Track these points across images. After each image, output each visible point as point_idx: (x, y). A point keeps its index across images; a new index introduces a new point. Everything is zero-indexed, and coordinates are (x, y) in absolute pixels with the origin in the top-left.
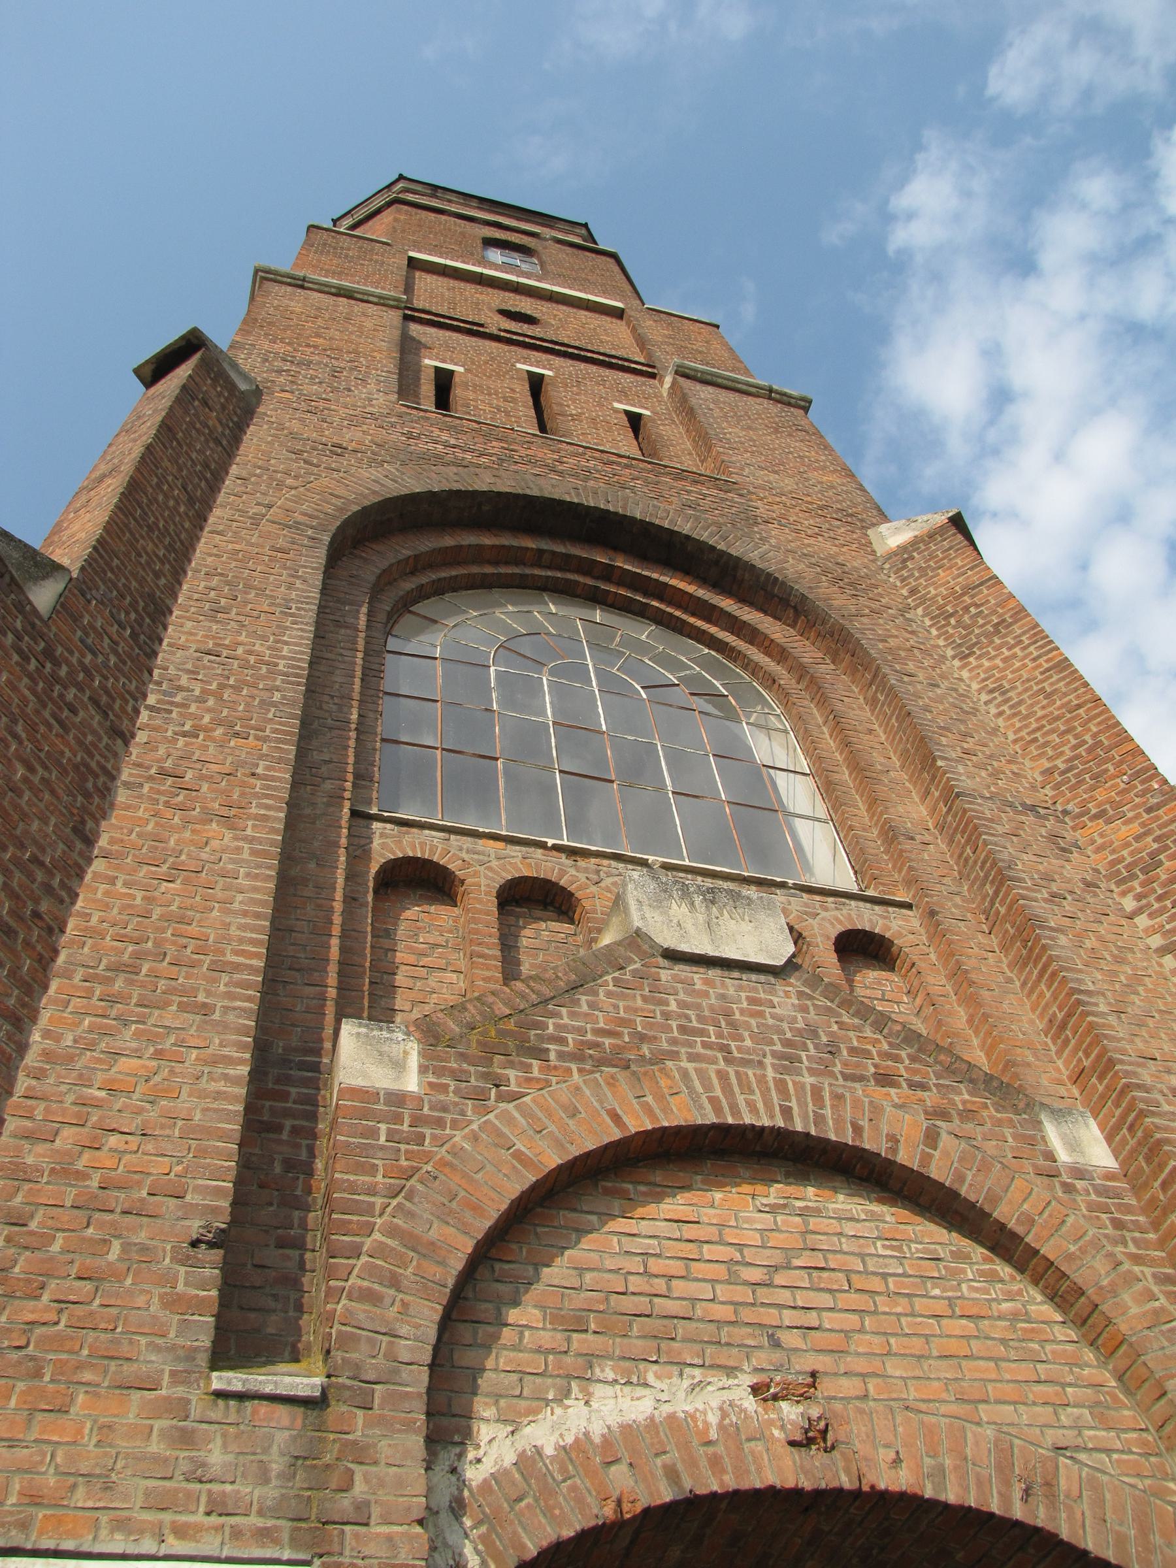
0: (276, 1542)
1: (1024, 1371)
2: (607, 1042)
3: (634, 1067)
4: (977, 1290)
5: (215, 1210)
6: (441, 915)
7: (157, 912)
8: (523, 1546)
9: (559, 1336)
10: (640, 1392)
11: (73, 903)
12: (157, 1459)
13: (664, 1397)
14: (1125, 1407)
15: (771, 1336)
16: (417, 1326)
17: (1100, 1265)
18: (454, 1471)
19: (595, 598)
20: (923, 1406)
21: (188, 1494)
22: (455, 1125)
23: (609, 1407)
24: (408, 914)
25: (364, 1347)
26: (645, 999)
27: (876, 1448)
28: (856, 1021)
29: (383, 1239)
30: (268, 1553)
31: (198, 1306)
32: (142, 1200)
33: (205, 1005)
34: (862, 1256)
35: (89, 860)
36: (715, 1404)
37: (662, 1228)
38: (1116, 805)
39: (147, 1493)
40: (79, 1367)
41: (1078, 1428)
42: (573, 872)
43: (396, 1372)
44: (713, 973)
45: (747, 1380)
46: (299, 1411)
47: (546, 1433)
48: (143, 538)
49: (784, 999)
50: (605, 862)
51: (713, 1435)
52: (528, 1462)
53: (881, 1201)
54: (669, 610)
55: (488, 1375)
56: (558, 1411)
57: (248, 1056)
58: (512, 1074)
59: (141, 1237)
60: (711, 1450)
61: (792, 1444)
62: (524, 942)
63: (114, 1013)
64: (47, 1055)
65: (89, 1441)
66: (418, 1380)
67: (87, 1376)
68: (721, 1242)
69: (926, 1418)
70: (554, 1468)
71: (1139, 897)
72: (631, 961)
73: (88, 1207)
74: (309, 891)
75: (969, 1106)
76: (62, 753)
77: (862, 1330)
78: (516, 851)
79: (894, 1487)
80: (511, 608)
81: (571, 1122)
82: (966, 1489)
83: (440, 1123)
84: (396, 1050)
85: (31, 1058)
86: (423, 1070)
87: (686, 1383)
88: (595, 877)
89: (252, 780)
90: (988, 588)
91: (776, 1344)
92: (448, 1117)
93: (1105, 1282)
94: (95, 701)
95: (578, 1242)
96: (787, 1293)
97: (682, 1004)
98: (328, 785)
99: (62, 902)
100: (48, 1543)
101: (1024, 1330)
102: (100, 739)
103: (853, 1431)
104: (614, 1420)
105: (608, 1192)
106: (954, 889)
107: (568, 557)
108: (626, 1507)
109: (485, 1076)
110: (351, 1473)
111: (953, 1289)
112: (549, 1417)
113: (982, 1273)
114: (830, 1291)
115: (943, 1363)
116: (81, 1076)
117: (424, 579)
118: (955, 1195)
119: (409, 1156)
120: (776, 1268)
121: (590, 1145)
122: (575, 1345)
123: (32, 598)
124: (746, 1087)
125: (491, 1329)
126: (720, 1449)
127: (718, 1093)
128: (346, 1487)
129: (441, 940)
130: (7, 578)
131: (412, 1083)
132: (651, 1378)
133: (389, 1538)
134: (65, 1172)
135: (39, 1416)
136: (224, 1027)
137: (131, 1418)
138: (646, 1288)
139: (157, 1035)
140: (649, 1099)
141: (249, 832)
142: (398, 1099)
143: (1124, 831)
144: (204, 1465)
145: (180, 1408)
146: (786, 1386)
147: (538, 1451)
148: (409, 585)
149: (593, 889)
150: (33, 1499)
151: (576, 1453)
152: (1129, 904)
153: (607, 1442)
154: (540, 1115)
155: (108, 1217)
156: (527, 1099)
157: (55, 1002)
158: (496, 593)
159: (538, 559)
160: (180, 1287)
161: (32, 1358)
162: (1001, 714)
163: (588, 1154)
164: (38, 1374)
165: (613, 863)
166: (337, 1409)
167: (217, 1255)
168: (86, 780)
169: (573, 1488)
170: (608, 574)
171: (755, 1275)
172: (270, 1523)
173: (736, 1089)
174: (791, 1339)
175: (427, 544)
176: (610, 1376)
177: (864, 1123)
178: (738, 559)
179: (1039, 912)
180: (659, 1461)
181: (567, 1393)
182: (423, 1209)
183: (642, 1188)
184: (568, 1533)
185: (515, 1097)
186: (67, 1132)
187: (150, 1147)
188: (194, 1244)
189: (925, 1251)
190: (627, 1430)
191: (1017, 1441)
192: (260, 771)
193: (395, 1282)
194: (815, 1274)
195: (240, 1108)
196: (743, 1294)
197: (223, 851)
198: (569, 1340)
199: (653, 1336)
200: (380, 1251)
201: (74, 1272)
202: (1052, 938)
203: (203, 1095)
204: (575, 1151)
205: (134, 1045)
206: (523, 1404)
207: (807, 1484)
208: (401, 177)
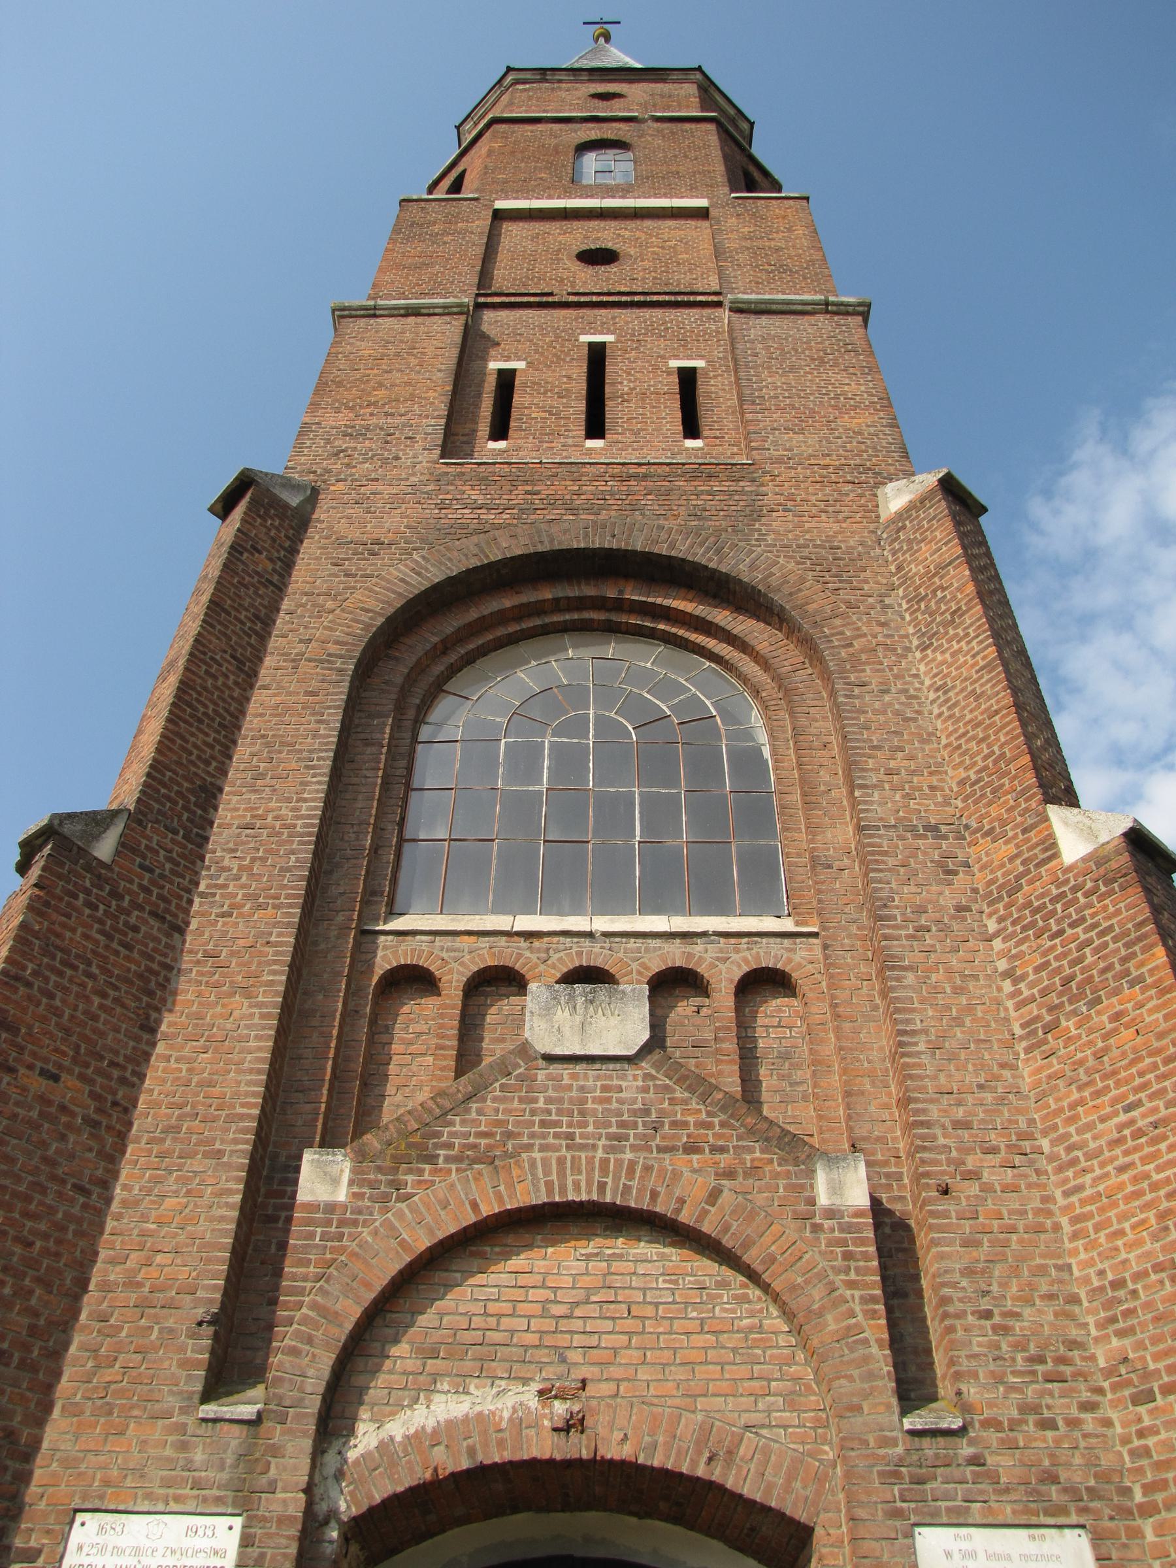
0: (224, 1504)
1: (743, 1371)
2: (483, 1142)
3: (497, 1162)
4: (726, 1310)
5: (211, 1301)
6: (429, 1005)
7: (195, 1079)
8: (373, 1497)
9: (419, 1362)
10: (463, 1397)
11: (143, 1082)
12: (169, 1459)
13: (478, 1400)
14: (815, 1394)
15: (561, 1355)
16: (318, 1370)
17: (817, 1292)
18: (340, 1453)
19: (612, 629)
20: (655, 1401)
21: (182, 1478)
22: (366, 1224)
23: (445, 1408)
24: (406, 1009)
25: (287, 1385)
26: (521, 1100)
27: (612, 1430)
28: (686, 1094)
29: (310, 1313)
30: (219, 1510)
31: (195, 1364)
32: (172, 1298)
33: (219, 1151)
34: (644, 1290)
35: (154, 1045)
36: (510, 1404)
37: (505, 1279)
38: (1003, 823)
39: (162, 1479)
40: (132, 1407)
41: (769, 1412)
42: (527, 954)
43: (303, 1399)
44: (579, 1068)
45: (535, 1387)
46: (245, 1427)
47: (397, 1428)
48: (193, 734)
49: (631, 1082)
50: (555, 940)
51: (504, 1425)
52: (384, 1446)
53: (673, 1244)
54: (674, 630)
55: (371, 1391)
56: (409, 1412)
57: (241, 1187)
58: (410, 1178)
59: (170, 1323)
60: (500, 1435)
61: (555, 1430)
62: (488, 1019)
63: (164, 1166)
64: (125, 1203)
65: (135, 1450)
66: (313, 1405)
67: (135, 1412)
68: (544, 1286)
69: (654, 1409)
70: (400, 1450)
71: (1000, 920)
72: (518, 1066)
73: (143, 1305)
74: (315, 1022)
75: (756, 1164)
76: (129, 970)
77: (628, 1347)
78: (484, 942)
79: (617, 1457)
80: (533, 663)
81: (442, 1213)
82: (668, 1457)
83: (355, 1223)
84: (335, 1169)
85: (115, 1207)
86: (351, 1183)
87: (495, 1390)
88: (544, 955)
89: (266, 949)
90: (955, 568)
91: (563, 1360)
92: (361, 1218)
93: (816, 1306)
94: (153, 914)
95: (445, 1294)
96: (580, 1322)
97: (549, 1100)
98: (340, 918)
99: (133, 1085)
100: (112, 1507)
101: (754, 1340)
102: (159, 942)
103: (599, 1423)
104: (442, 1417)
105: (473, 1255)
106: (854, 916)
107: (581, 599)
108: (440, 1472)
109: (391, 1183)
110: (269, 1463)
111: (708, 1311)
112: (402, 1416)
113: (735, 1297)
114: (613, 1318)
115: (682, 1368)
116: (142, 1215)
117: (452, 657)
118: (719, 1243)
119: (333, 1250)
120: (578, 1304)
121: (452, 1230)
122: (427, 1368)
123: (96, 854)
124: (576, 1169)
125: (376, 1360)
126: (507, 1435)
127: (554, 1177)
128: (266, 1471)
129: (425, 1028)
130: (75, 849)
131: (342, 1195)
132: (472, 1389)
133: (284, 1501)
134: (132, 1284)
135: (111, 1437)
136: (228, 1166)
137: (157, 1436)
138: (483, 1325)
139: (188, 1178)
140: (502, 1188)
141: (260, 999)
142: (331, 1207)
143: (1005, 850)
144: (191, 1461)
145: (182, 1428)
146: (563, 1389)
147: (392, 1438)
148: (438, 669)
149: (542, 967)
150: (106, 1483)
151: (415, 1439)
152: (992, 926)
153: (435, 1431)
154: (423, 1210)
155: (152, 1311)
156: (416, 1198)
157: (129, 1162)
158: (523, 648)
159: (557, 605)
160: (189, 1353)
161: (108, 1404)
162: (940, 715)
163: (452, 1236)
164: (110, 1413)
165: (562, 939)
166: (267, 1424)
167: (212, 1329)
168: (150, 981)
169: (409, 1462)
170: (620, 605)
171: (558, 1310)
172: (223, 1493)
173: (569, 1172)
174: (574, 1356)
175: (451, 624)
176: (446, 1387)
177: (661, 1190)
178: (727, 575)
179: (896, 951)
180: (465, 1444)
181: (416, 1400)
182: (334, 1288)
183: (497, 1249)
184: (400, 1489)
185: (409, 1197)
186: (133, 1255)
187: (179, 1261)
188: (200, 1324)
189: (696, 1282)
190: (450, 1423)
191: (717, 1423)
192: (273, 939)
193: (310, 1341)
194: (605, 1306)
195: (233, 1226)
196: (548, 1324)
197: (241, 1019)
198: (424, 1365)
199: (482, 1359)
200: (305, 1320)
201: (132, 1348)
202: (898, 979)
203: (211, 1219)
204: (441, 1235)
205: (174, 1188)
206: (388, 1408)
207: (558, 1456)
208: (509, 69)
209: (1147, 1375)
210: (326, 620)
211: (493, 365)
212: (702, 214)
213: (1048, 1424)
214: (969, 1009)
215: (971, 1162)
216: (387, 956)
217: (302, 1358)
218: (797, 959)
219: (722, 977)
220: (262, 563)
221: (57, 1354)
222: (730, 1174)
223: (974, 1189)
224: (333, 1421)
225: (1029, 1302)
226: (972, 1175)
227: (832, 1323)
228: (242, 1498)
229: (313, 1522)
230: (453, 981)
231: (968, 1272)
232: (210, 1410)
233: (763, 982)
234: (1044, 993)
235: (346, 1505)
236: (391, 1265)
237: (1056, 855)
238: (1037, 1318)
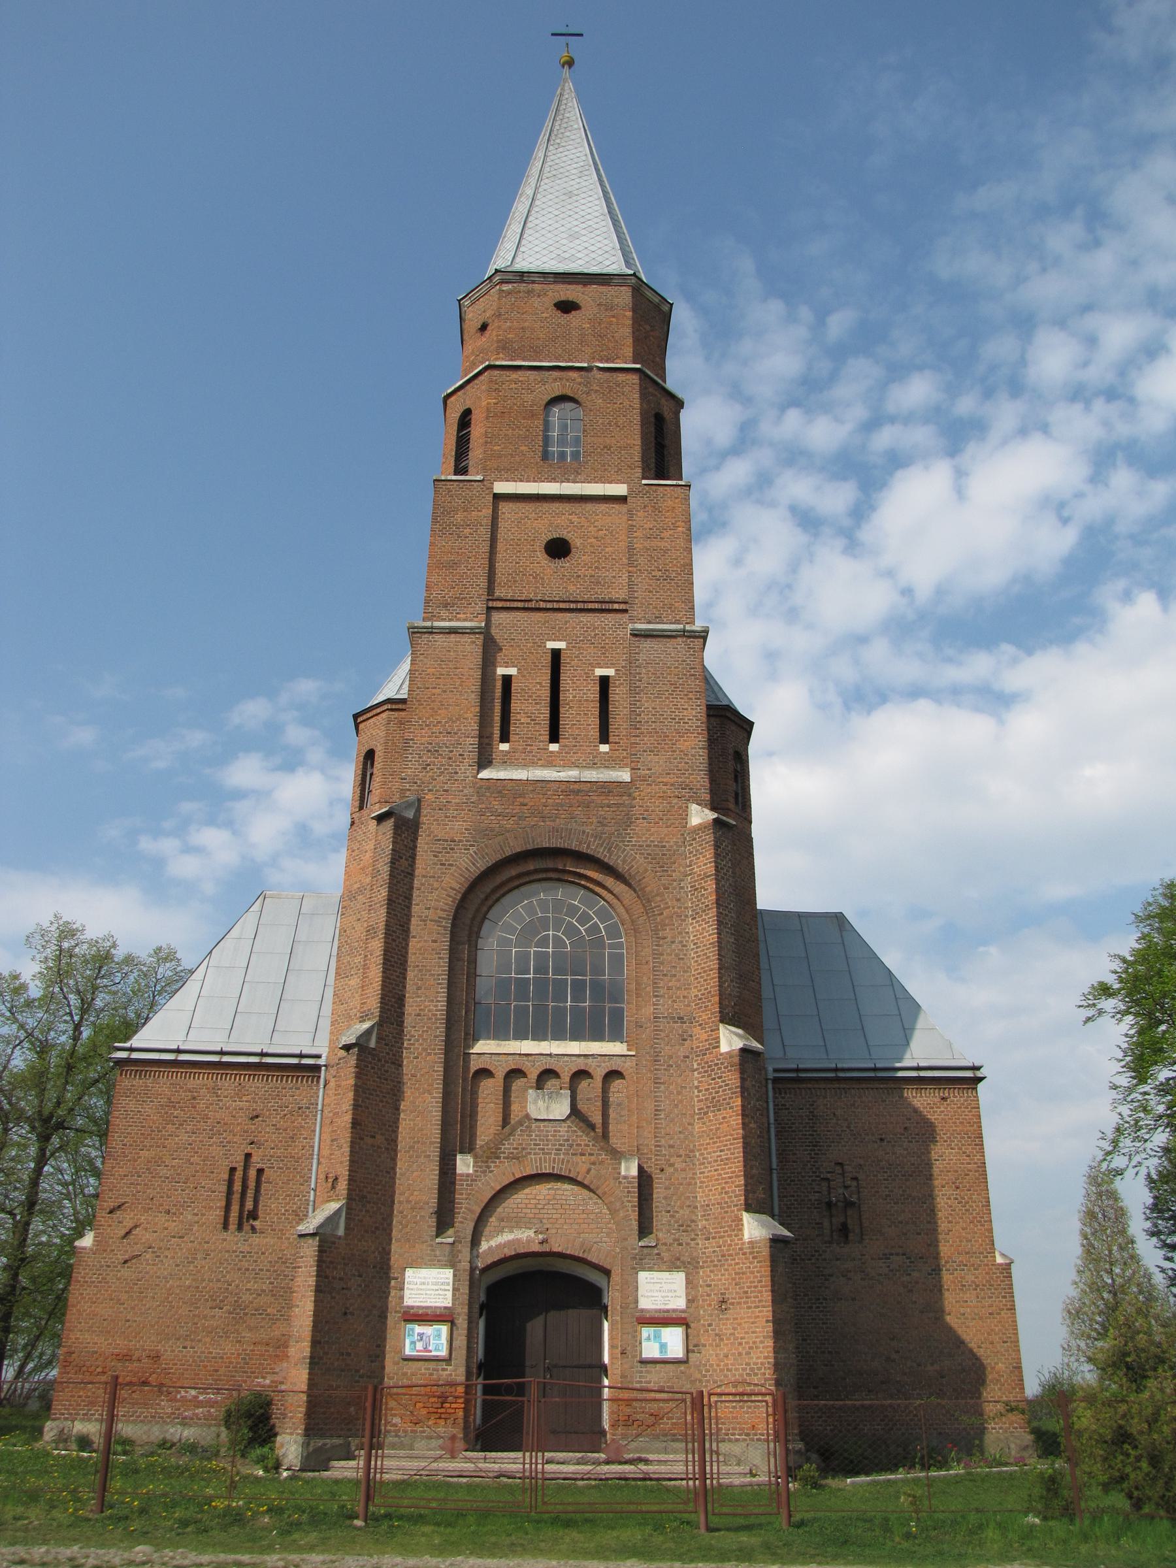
6: (491, 1080)
23: (507, 1237)
47: (493, 1243)
49: (563, 1128)
52: (490, 1248)
66: (469, 1238)
73: (413, 1209)
78: (510, 1058)
103: (552, 1241)
131: (471, 1171)
142: (468, 1175)
151: (499, 1246)
159: (536, 871)
199: (517, 1222)
209: (710, 1233)
210: (435, 895)
211: (501, 671)
212: (622, 499)
213: (681, 1244)
214: (681, 1101)
215: (672, 1160)
216: (474, 1067)
217: (464, 1222)
218: (626, 1067)
219: (599, 1073)
220: (404, 863)
221: (390, 1224)
222: (594, 1163)
223: (672, 1170)
225: (682, 1207)
226: (672, 1165)
227: (622, 1214)
228: (452, 1264)
229: (472, 1270)
230: (500, 1074)
231: (665, 1198)
232: (438, 1240)
233: (613, 1075)
234: (706, 1099)
235: (480, 1265)
237: (718, 1047)
238: (684, 1213)
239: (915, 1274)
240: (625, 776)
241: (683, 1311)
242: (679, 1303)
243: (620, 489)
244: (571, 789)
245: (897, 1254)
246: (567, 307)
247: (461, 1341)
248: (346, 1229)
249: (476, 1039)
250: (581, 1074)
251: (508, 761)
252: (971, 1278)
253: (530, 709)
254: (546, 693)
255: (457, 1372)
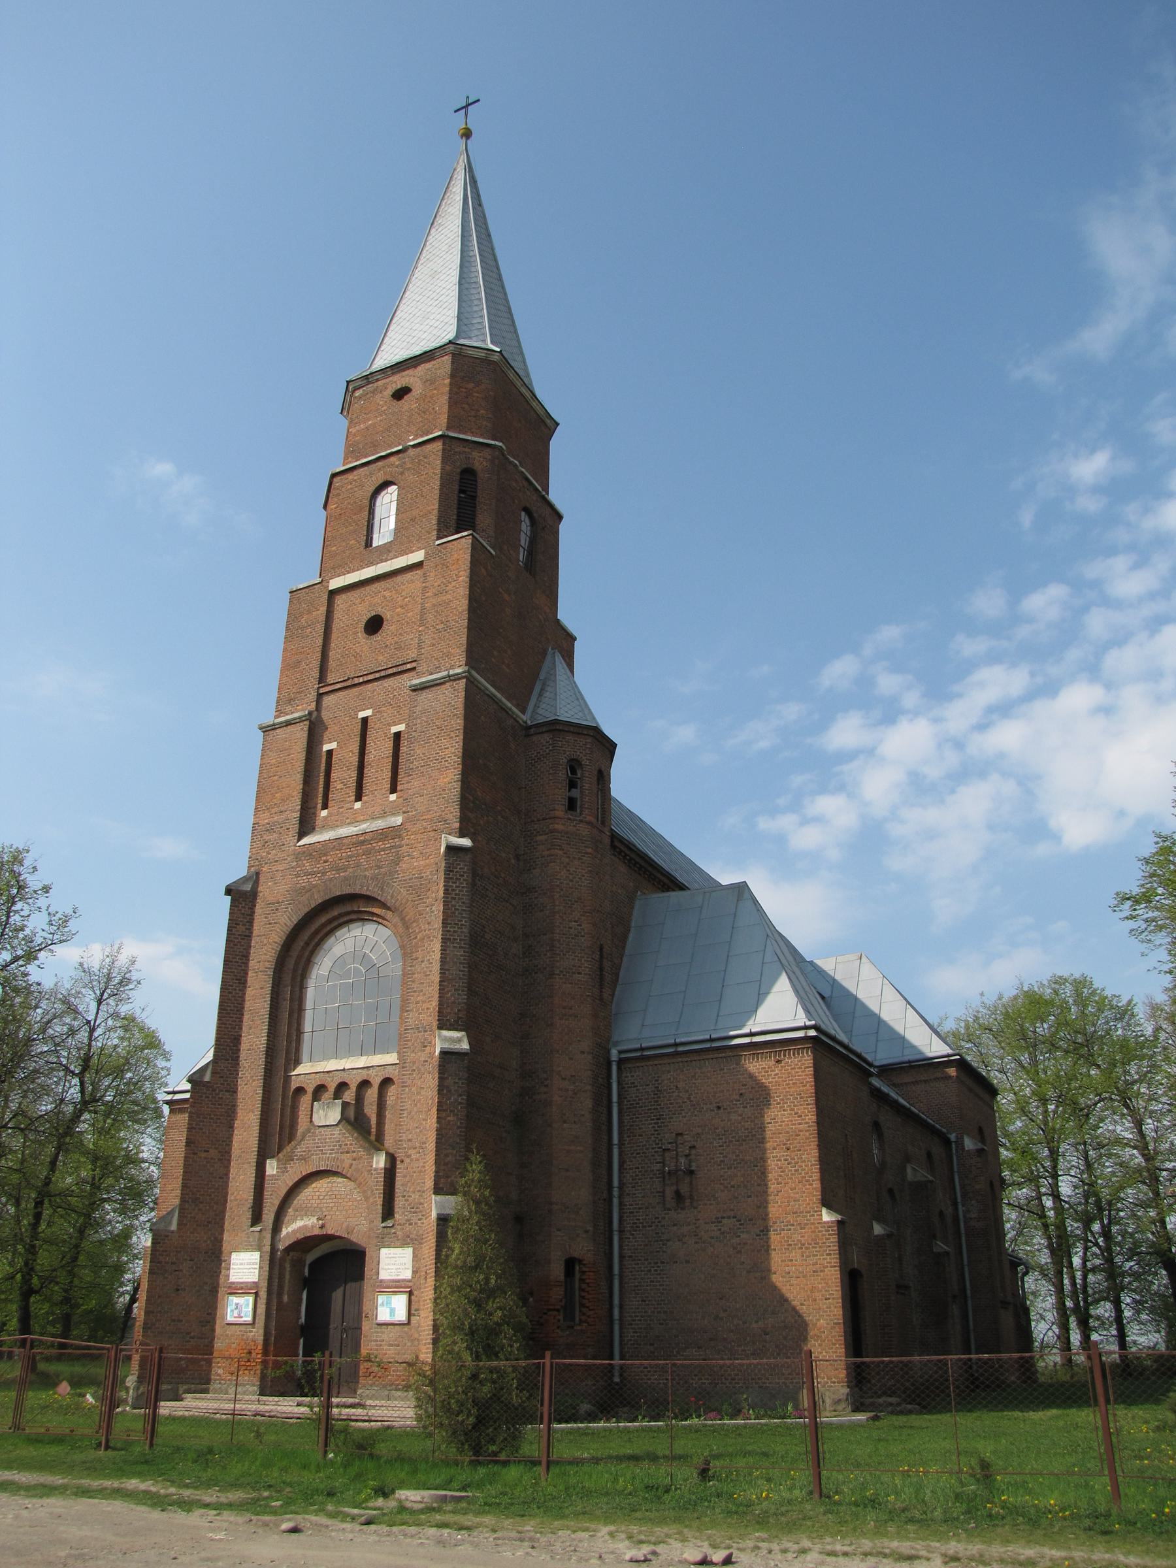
23: (299, 1224)
47: (290, 1229)
49: (337, 1131)
73: (238, 1205)
103: (327, 1226)
142: (273, 1176)
148: (307, 954)
199: (306, 1211)
208: (348, 382)
211: (326, 747)
217: (268, 1217)
220: (241, 928)
221: (223, 1219)
224: (276, 1228)
228: (259, 1248)
233: (387, 1082)
235: (281, 1246)
236: (284, 1191)
239: (744, 1236)
240: (398, 820)
241: (409, 1281)
242: (407, 1274)
243: (418, 556)
244: (360, 841)
245: (729, 1217)
246: (400, 394)
247: (262, 1309)
248: (179, 1225)
249: (297, 1062)
250: (342, 1086)
251: (327, 826)
252: (796, 1237)
253: (344, 776)
254: (354, 760)
255: (258, 1333)
